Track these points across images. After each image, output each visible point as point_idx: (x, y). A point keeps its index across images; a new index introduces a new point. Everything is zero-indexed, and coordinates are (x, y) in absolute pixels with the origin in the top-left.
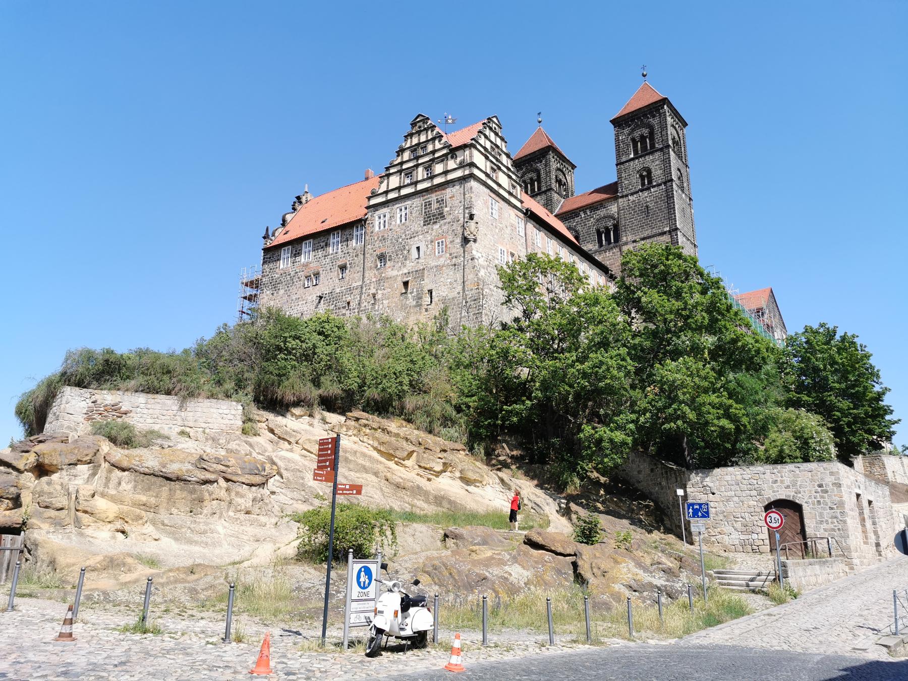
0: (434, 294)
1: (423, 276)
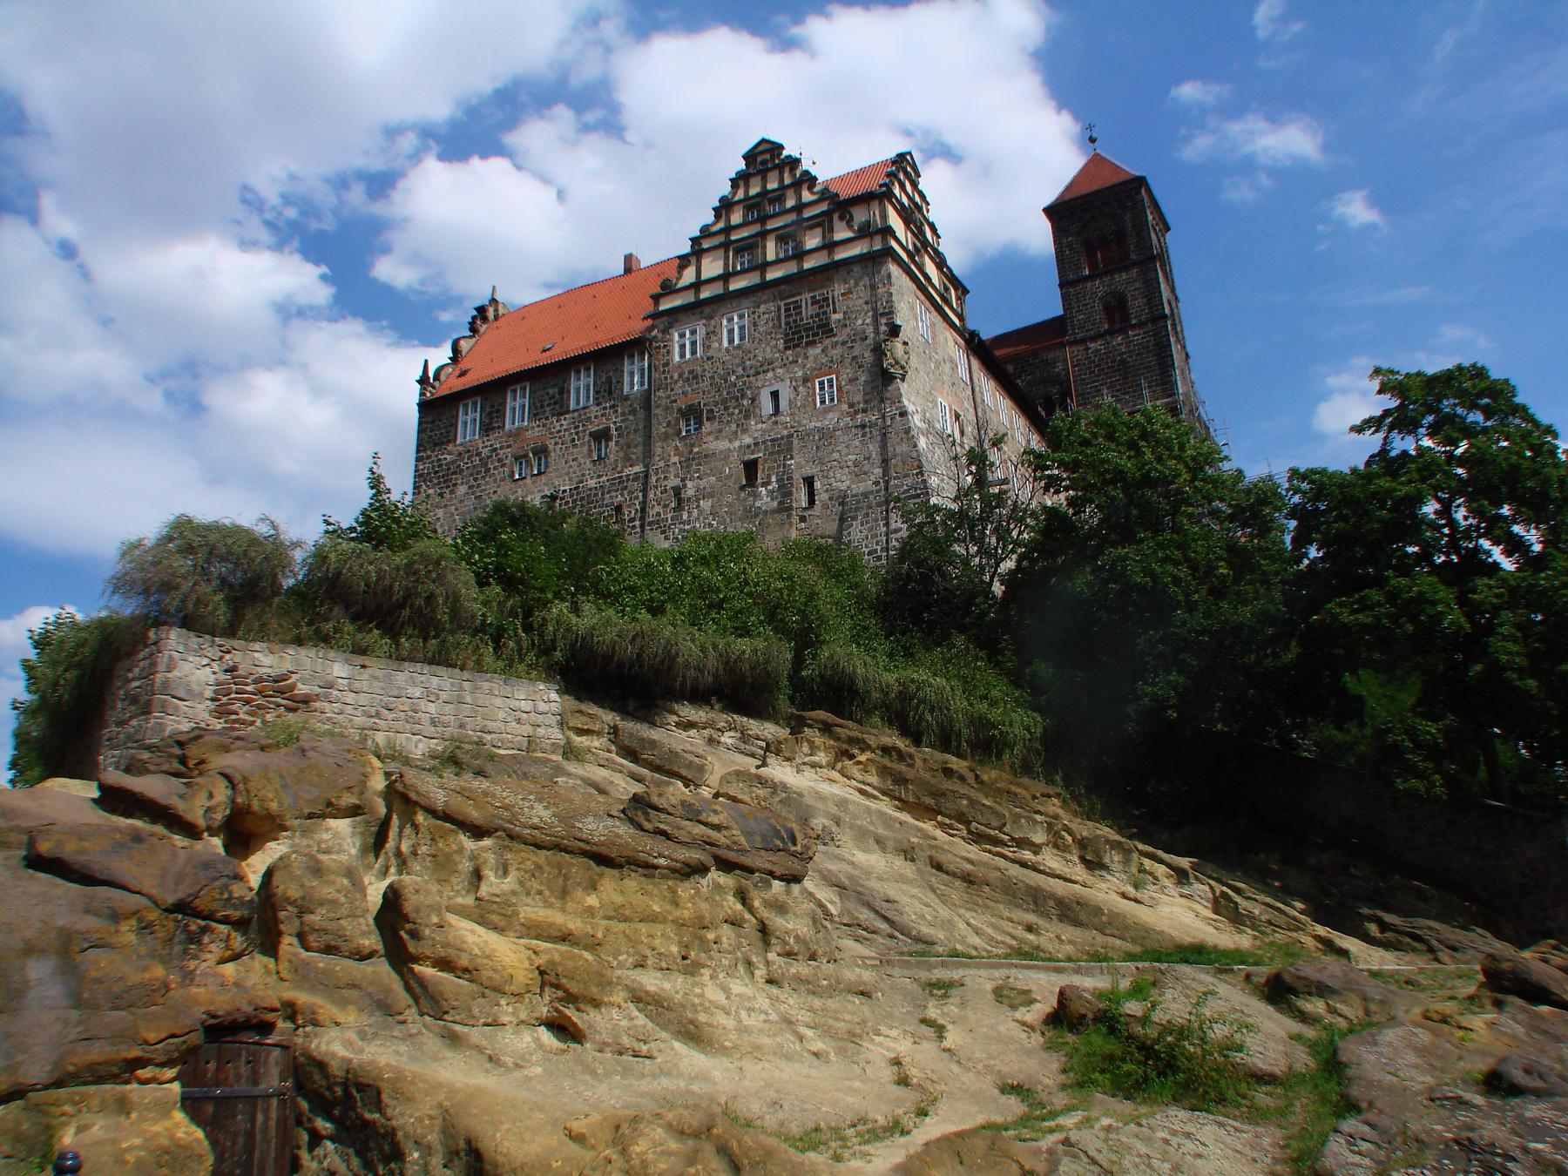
0: (817, 485)
1: (790, 450)
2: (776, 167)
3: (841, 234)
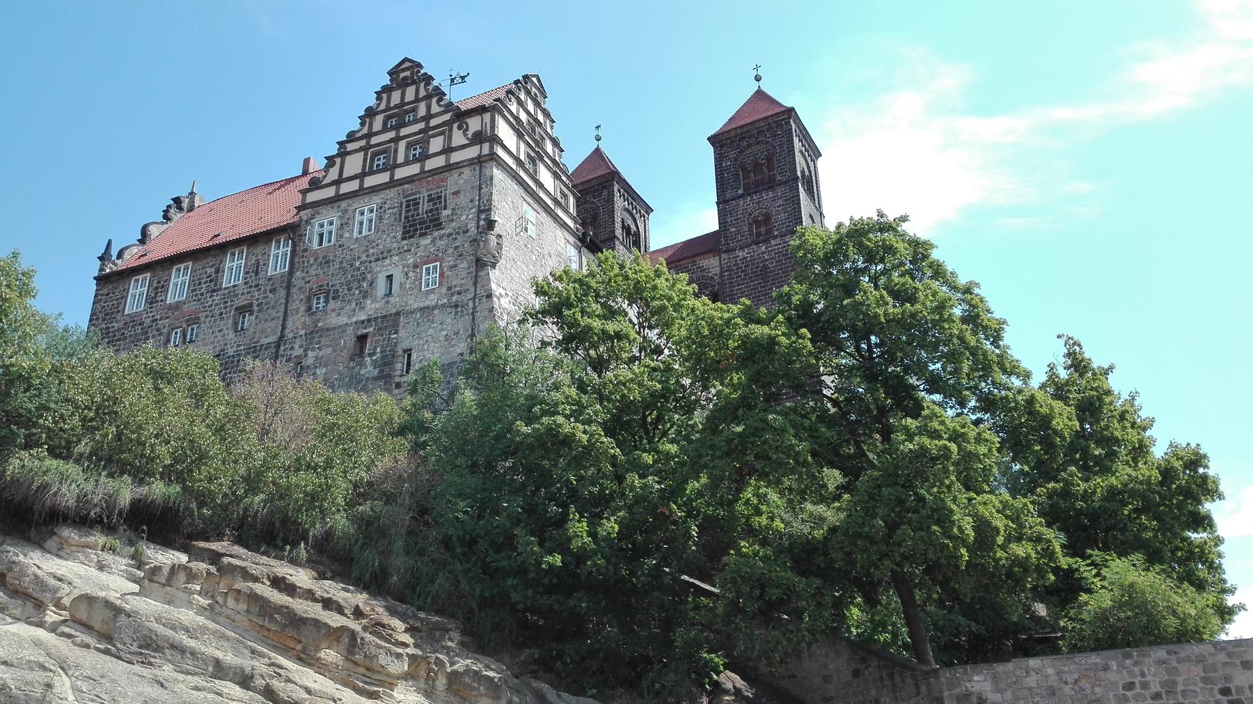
0: (414, 356)
2: (414, 82)
3: (458, 138)
